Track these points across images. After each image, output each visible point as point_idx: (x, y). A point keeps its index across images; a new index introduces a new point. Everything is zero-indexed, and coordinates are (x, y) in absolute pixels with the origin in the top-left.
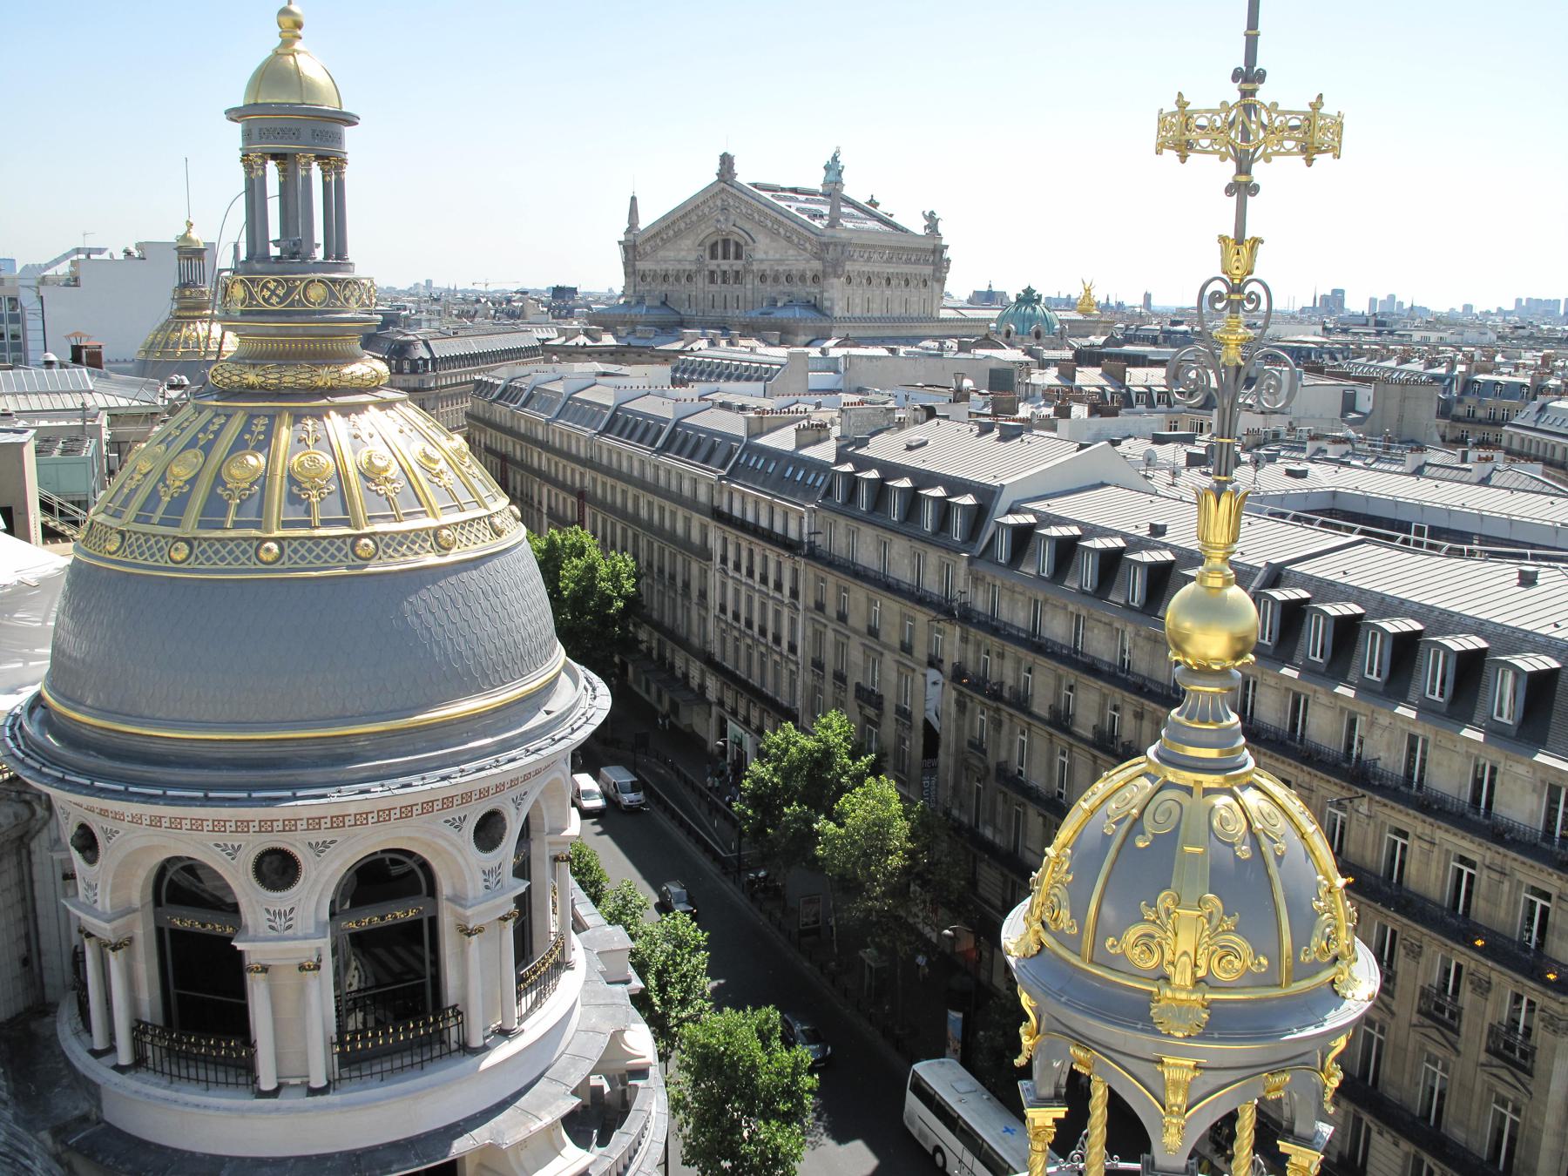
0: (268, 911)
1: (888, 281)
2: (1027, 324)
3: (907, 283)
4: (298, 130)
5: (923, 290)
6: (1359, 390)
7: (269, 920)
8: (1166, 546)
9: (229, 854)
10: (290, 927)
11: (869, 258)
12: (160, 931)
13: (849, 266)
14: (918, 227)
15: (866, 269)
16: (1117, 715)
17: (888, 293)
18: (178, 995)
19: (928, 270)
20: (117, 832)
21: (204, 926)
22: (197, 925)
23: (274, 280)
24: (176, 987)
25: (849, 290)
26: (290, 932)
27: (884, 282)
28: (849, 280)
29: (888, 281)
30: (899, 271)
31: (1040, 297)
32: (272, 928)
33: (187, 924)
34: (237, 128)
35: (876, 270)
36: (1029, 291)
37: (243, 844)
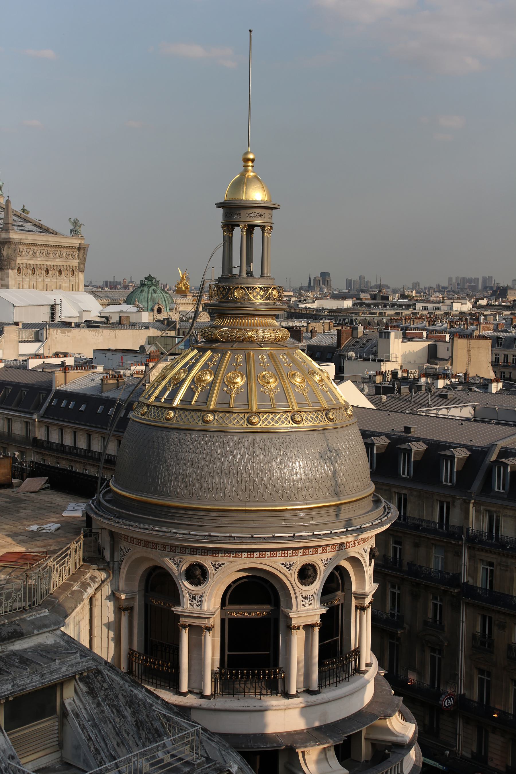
0: (302, 596)
1: (47, 271)
2: (150, 304)
3: (60, 271)
4: (264, 214)
5: (71, 278)
6: (438, 344)
7: (303, 601)
8: (419, 439)
9: (287, 568)
10: (311, 604)
11: (34, 253)
12: (223, 621)
13: (18, 261)
14: (66, 228)
15: (31, 262)
16: (398, 547)
17: (47, 280)
18: (228, 654)
19: (75, 263)
20: (224, 564)
21: (250, 614)
22: (246, 615)
23: (259, 288)
24: (228, 651)
25: (19, 278)
26: (311, 606)
27: (44, 272)
28: (19, 271)
29: (47, 271)
30: (55, 263)
31: (158, 282)
32: (303, 605)
33: (240, 615)
34: (221, 210)
35: (38, 263)
36: (149, 278)
37: (294, 562)
